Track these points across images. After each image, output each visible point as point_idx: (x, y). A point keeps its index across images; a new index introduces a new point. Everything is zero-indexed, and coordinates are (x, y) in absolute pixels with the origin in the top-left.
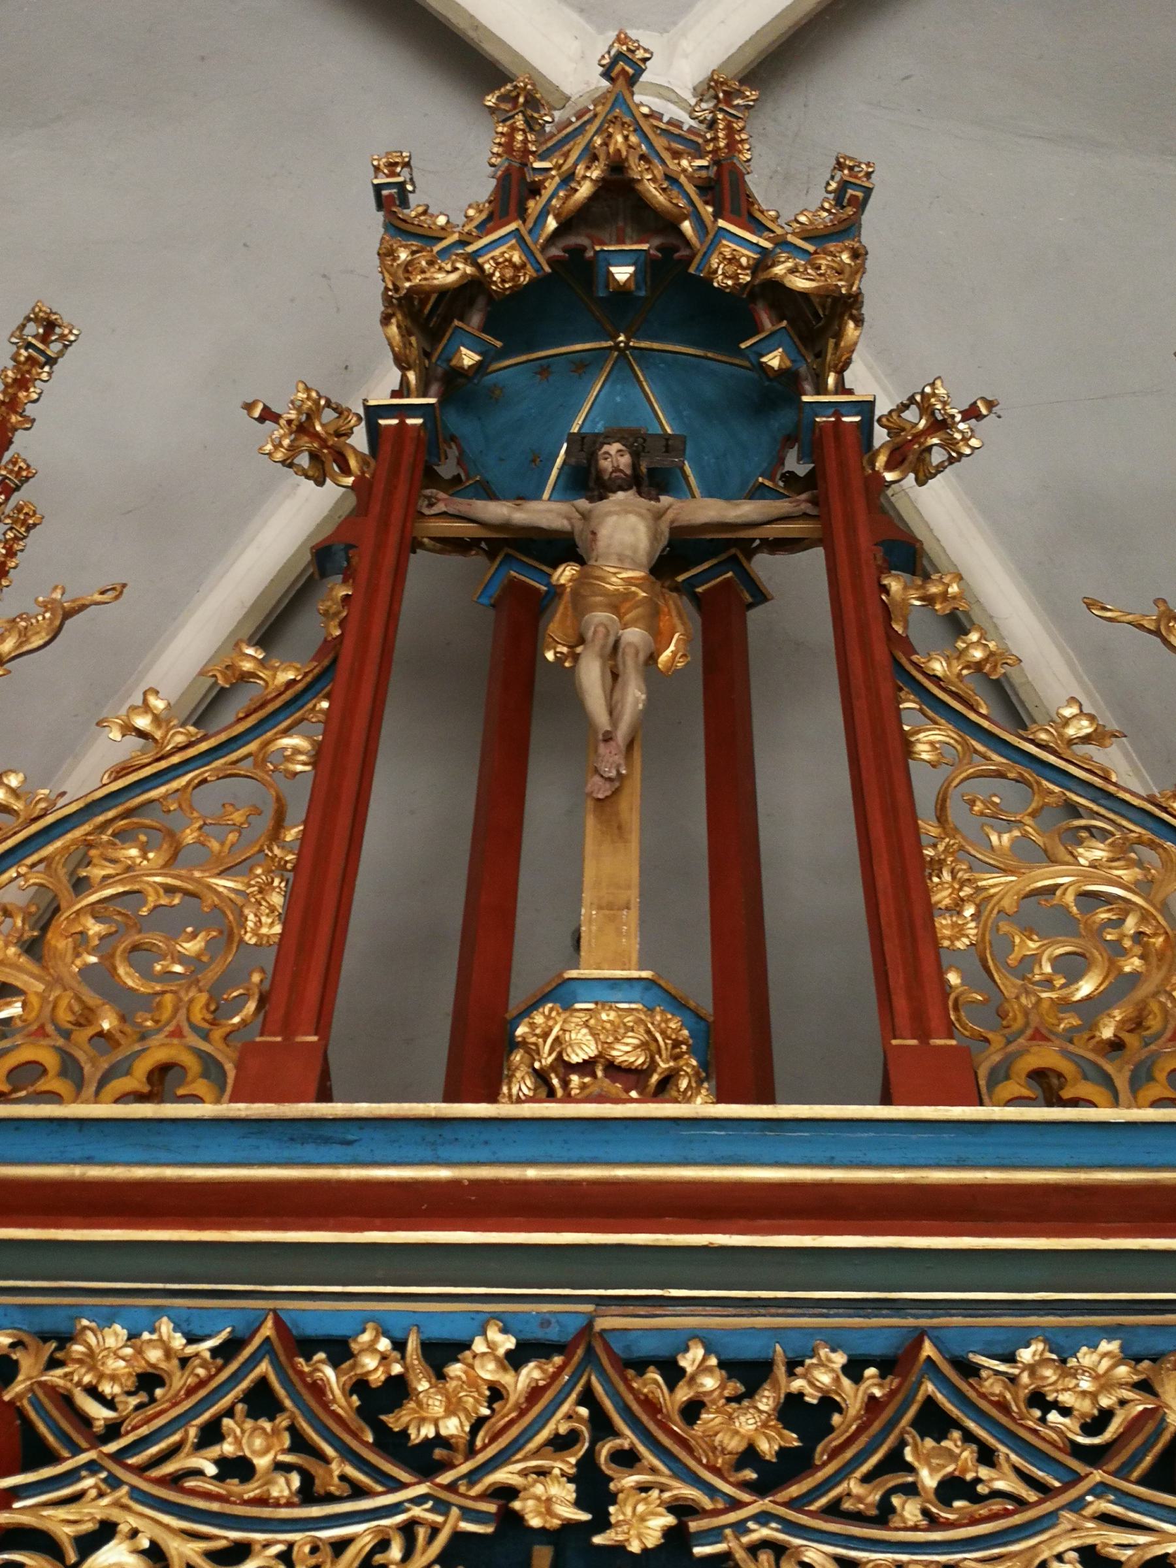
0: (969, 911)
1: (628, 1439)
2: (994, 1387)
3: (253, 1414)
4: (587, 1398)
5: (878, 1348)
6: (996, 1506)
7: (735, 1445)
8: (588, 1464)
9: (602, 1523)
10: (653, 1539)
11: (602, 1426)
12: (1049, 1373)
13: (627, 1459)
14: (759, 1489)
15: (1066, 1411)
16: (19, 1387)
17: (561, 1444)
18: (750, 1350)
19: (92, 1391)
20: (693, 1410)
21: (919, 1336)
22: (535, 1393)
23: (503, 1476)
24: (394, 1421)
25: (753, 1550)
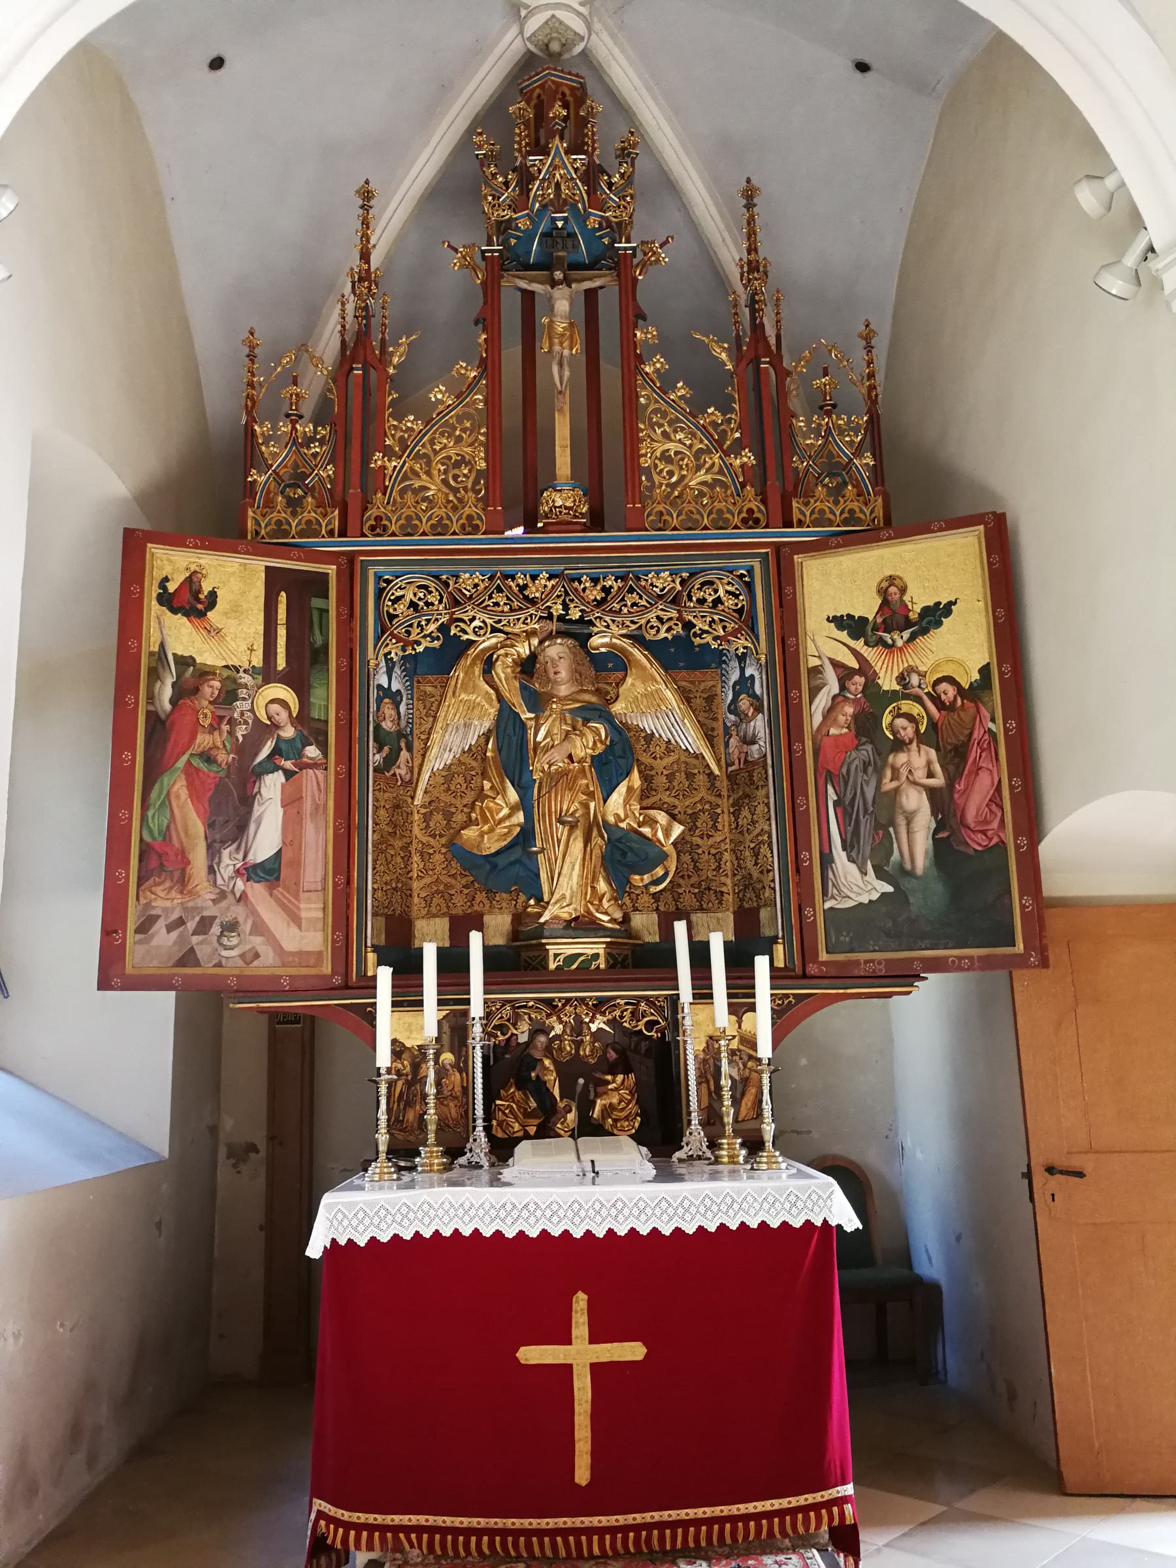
0: (649, 455)
1: (572, 597)
2: (643, 583)
3: (498, 592)
4: (564, 586)
5: (621, 575)
6: (641, 609)
7: (593, 598)
8: (564, 600)
9: (567, 614)
10: (577, 617)
11: (567, 594)
12: (654, 580)
13: (572, 601)
14: (597, 606)
15: (657, 587)
16: (451, 588)
17: (558, 596)
18: (594, 576)
19: (465, 589)
20: (584, 590)
21: (629, 572)
22: (553, 587)
23: (548, 604)
24: (526, 593)
25: (596, 618)
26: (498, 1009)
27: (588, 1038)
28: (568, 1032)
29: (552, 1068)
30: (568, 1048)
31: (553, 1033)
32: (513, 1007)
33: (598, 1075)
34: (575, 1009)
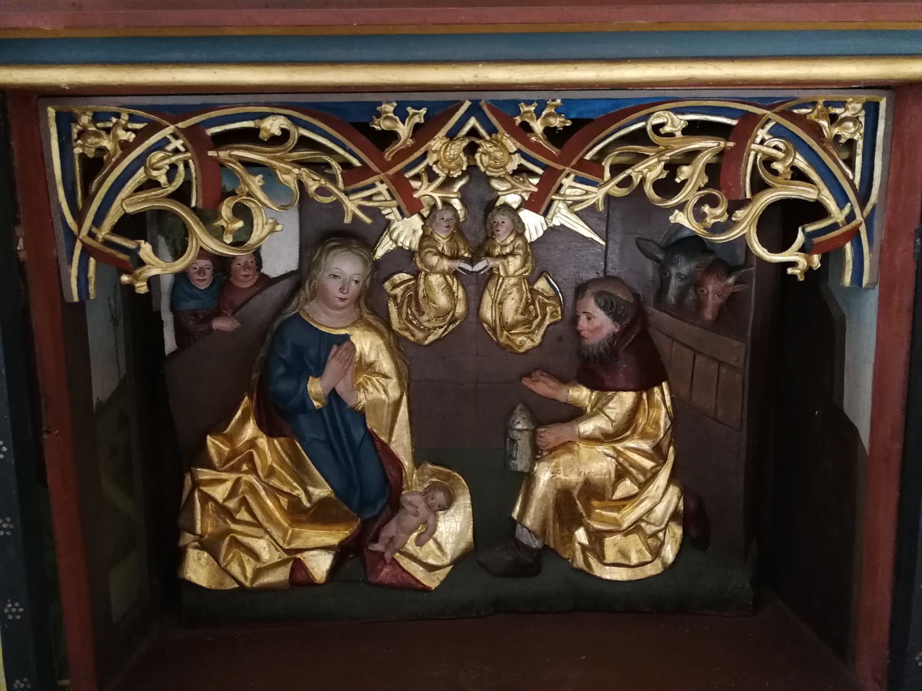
26: (126, 147)
27: (514, 263)
28: (443, 243)
29: (386, 365)
30: (442, 300)
31: (384, 247)
32: (193, 135)
33: (544, 387)
34: (471, 150)
